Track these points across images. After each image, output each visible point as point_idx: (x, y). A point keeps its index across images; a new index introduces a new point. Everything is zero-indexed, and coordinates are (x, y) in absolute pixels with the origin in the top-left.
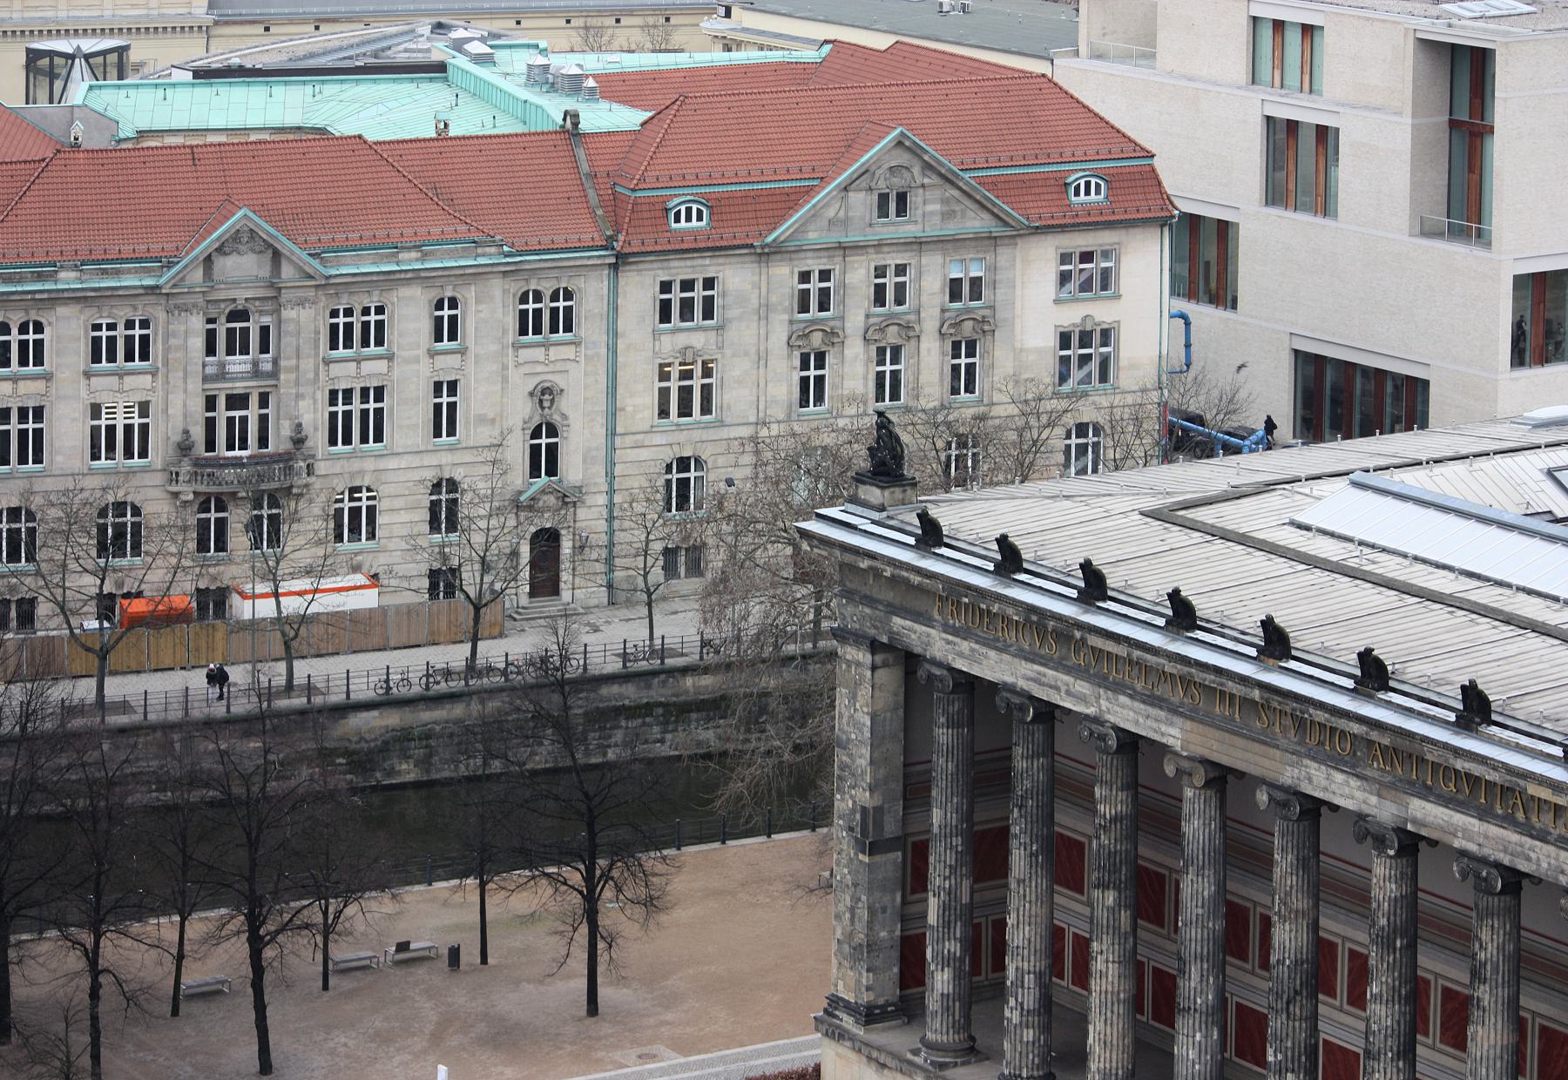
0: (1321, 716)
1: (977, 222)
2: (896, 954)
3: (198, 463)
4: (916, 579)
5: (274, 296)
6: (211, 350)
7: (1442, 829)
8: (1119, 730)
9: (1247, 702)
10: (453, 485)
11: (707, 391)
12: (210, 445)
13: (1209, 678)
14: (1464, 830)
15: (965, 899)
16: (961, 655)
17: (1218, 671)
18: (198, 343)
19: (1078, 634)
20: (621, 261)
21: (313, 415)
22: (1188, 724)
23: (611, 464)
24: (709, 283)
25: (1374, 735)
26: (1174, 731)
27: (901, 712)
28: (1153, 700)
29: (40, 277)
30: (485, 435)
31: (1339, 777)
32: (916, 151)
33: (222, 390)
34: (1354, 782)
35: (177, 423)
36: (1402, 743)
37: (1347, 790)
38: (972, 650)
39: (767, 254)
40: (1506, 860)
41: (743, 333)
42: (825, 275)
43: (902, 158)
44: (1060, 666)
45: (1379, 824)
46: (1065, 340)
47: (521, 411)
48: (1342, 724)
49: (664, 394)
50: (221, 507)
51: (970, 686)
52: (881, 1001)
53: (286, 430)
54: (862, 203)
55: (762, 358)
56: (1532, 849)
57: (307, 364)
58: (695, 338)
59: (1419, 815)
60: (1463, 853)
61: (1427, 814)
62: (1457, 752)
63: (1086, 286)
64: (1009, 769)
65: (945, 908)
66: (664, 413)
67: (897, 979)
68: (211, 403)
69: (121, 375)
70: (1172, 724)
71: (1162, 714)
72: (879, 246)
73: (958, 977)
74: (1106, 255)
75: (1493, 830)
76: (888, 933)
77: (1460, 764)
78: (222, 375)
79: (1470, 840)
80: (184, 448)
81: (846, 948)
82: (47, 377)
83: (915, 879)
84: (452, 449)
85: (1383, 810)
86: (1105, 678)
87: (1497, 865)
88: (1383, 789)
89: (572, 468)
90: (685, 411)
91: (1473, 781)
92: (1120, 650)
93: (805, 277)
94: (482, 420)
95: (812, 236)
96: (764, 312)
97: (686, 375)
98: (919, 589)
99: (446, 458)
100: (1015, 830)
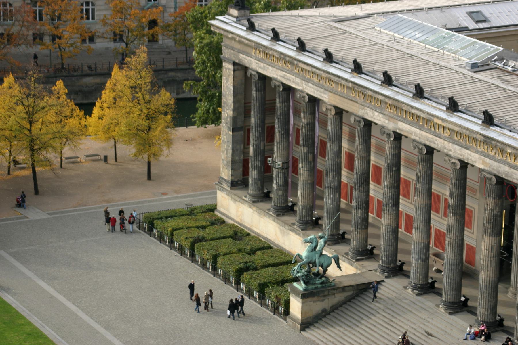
0: (370, 93)
2: (241, 165)
4: (246, 42)
7: (408, 132)
8: (308, 95)
9: (348, 87)
13: (336, 79)
14: (415, 133)
15: (262, 148)
16: (260, 67)
17: (339, 77)
19: (296, 62)
22: (330, 94)
25: (387, 100)
26: (326, 96)
27: (243, 86)
28: (318, 86)
31: (376, 114)
34: (381, 116)
36: (396, 104)
37: (379, 118)
38: (264, 66)
40: (428, 143)
44: (291, 72)
45: (389, 130)
48: (377, 96)
51: (264, 79)
52: (236, 180)
56: (436, 140)
59: (401, 127)
60: (414, 141)
61: (403, 127)
62: (412, 107)
64: (275, 106)
65: (255, 151)
67: (241, 173)
70: (325, 93)
71: (322, 90)
73: (259, 173)
75: (424, 133)
76: (239, 158)
77: (413, 111)
79: (417, 136)
81: (225, 162)
83: (247, 142)
85: (391, 125)
86: (305, 77)
87: (425, 145)
88: (390, 118)
91: (418, 117)
92: (309, 68)
98: (247, 45)
100: (276, 126)
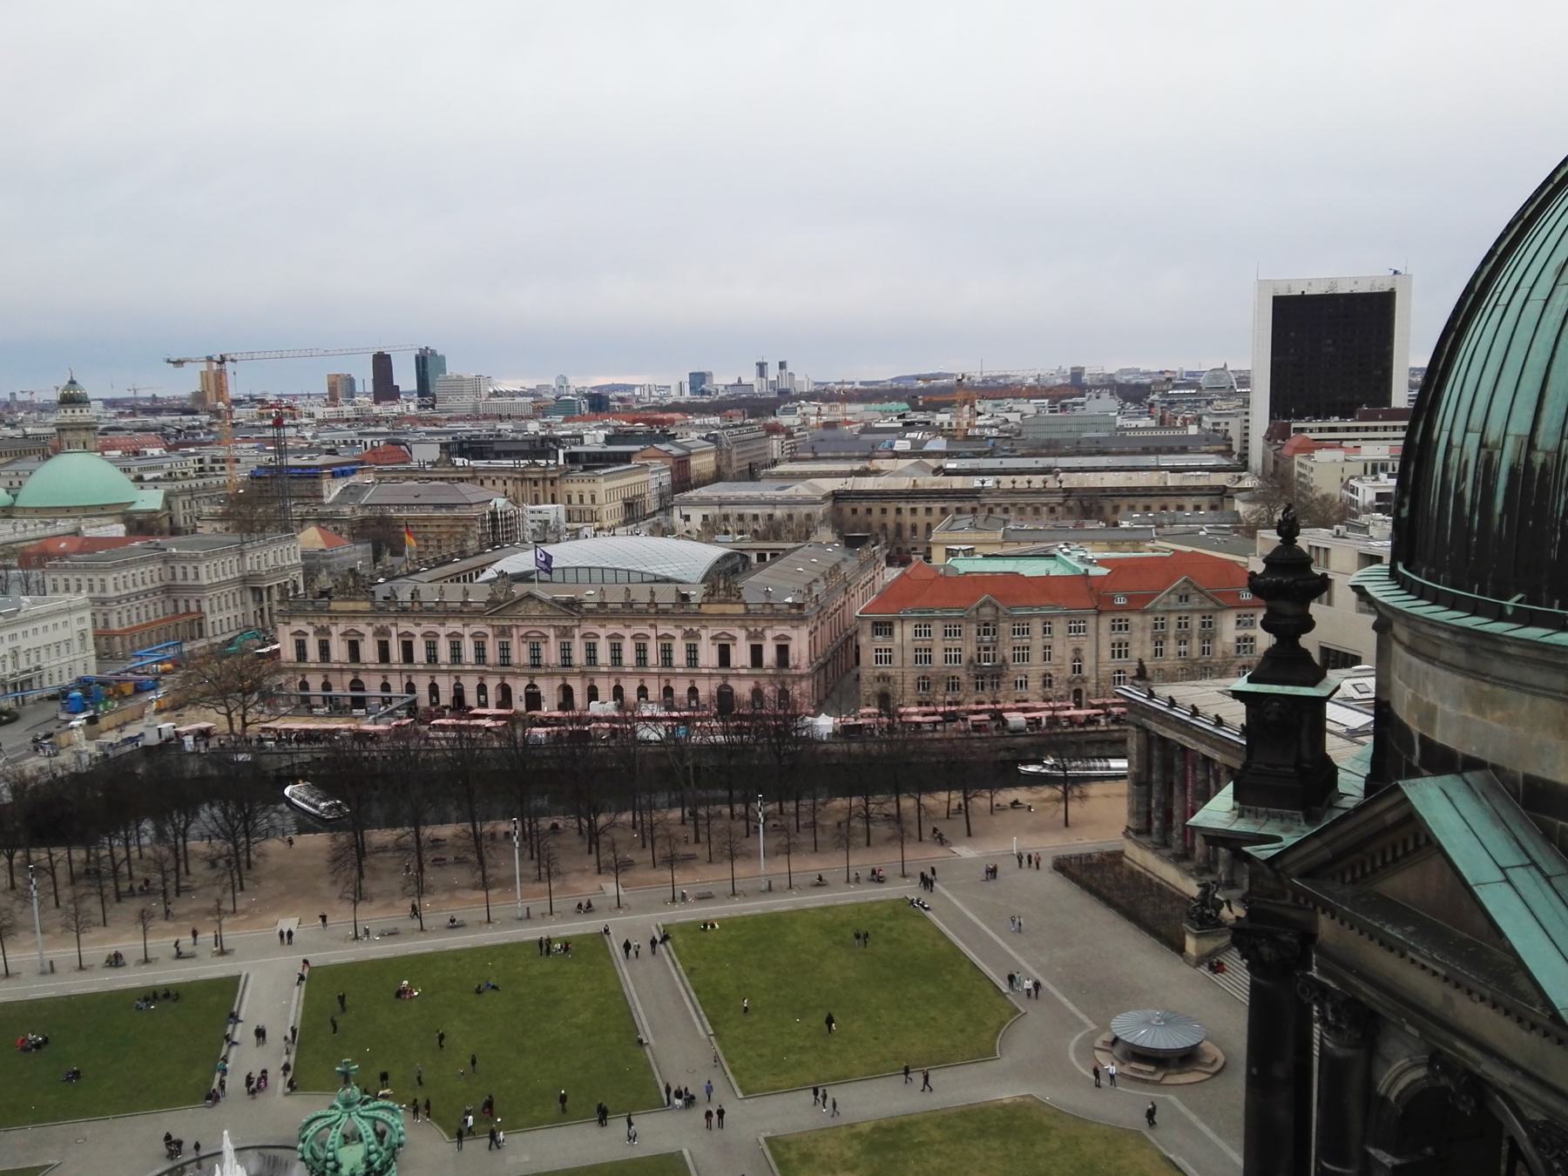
1: (1210, 605)
3: (976, 667)
5: (997, 619)
6: (979, 634)
10: (1050, 675)
11: (1126, 651)
12: (979, 661)
18: (975, 632)
20: (1099, 613)
21: (1008, 653)
23: (1097, 671)
24: (1127, 620)
29: (930, 612)
30: (1058, 661)
32: (1191, 583)
33: (982, 645)
35: (969, 654)
39: (1145, 612)
41: (1138, 635)
42: (1163, 619)
43: (1185, 585)
46: (1239, 640)
47: (1069, 655)
49: (1113, 651)
50: (982, 678)
53: (1001, 657)
54: (1173, 598)
55: (1143, 642)
57: (1007, 640)
58: (1123, 636)
63: (1246, 625)
66: (1113, 657)
68: (979, 649)
69: (953, 640)
72: (1180, 611)
74: (1252, 616)
78: (982, 641)
80: (971, 661)
82: (932, 640)
84: (1049, 665)
89: (1086, 672)
90: (1120, 657)
93: (1156, 619)
94: (1058, 657)
95: (1159, 607)
96: (1144, 629)
97: (1120, 645)
99: (1048, 667)
